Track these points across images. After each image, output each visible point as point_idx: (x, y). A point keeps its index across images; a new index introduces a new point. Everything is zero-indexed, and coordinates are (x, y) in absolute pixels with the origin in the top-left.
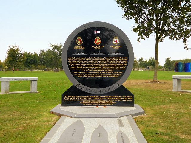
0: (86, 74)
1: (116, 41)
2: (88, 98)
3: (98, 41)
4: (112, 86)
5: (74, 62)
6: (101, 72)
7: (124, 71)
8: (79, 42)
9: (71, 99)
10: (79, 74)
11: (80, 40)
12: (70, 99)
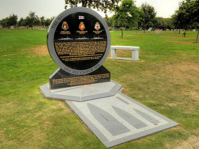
0: (72, 58)
1: (97, 27)
2: (75, 79)
3: (82, 26)
4: (95, 66)
5: (61, 47)
6: (85, 55)
7: (103, 53)
8: (65, 27)
9: (59, 82)
10: (66, 58)
11: (66, 25)
12: (58, 82)
